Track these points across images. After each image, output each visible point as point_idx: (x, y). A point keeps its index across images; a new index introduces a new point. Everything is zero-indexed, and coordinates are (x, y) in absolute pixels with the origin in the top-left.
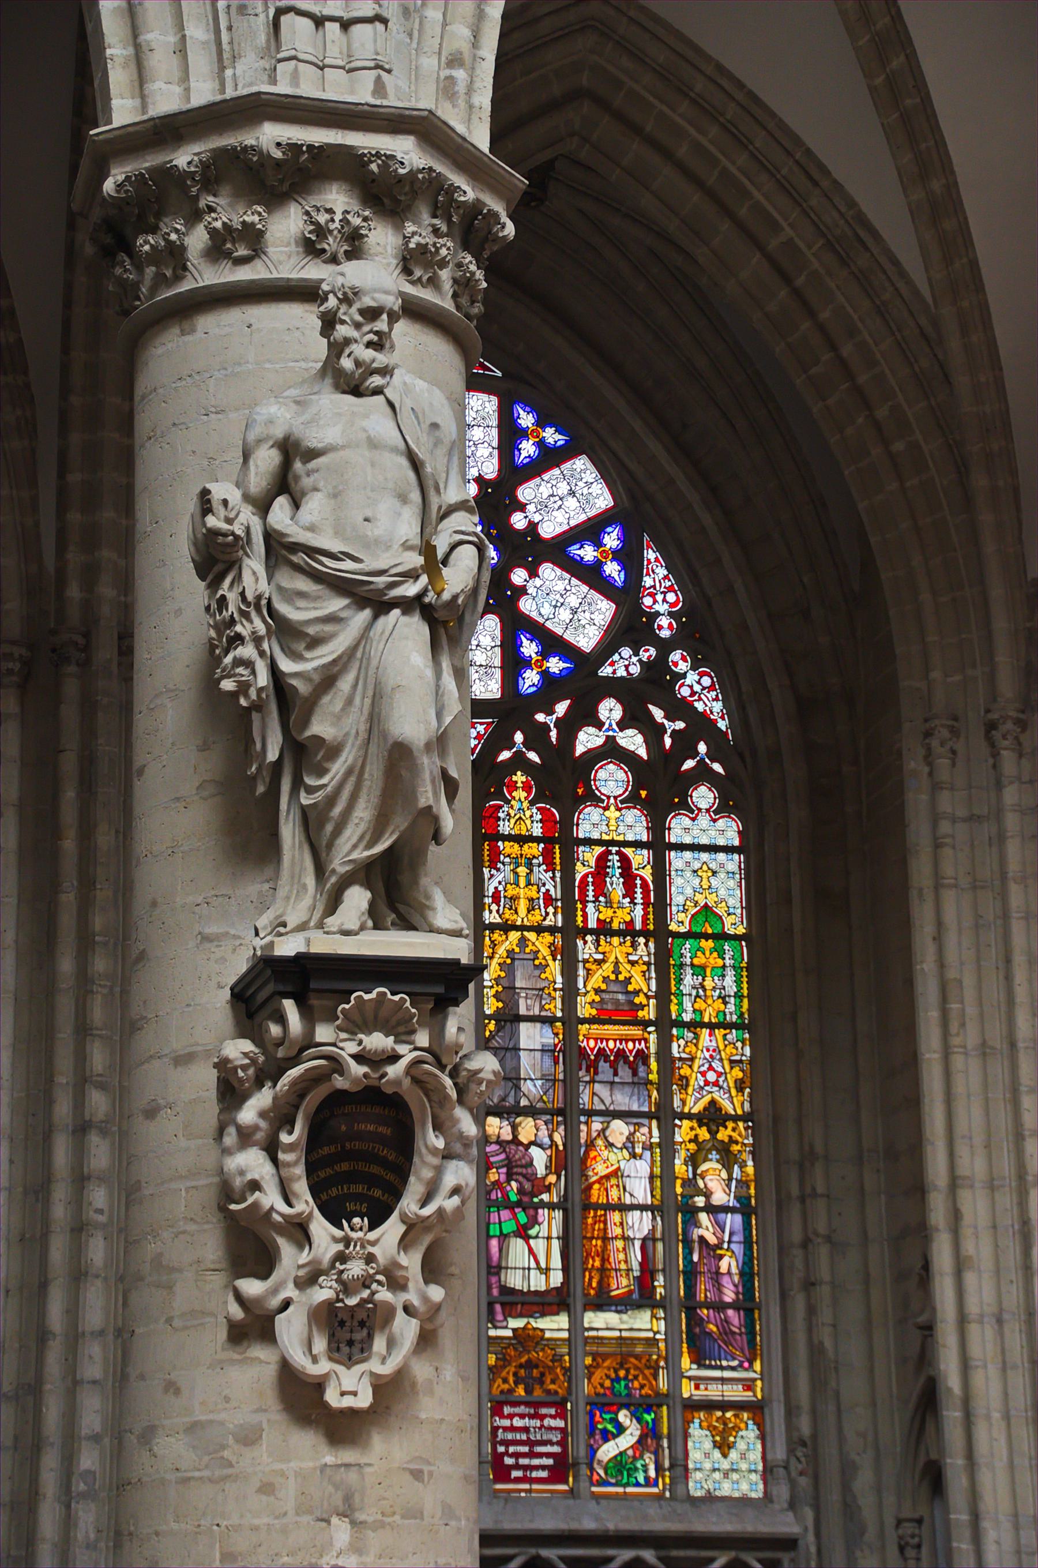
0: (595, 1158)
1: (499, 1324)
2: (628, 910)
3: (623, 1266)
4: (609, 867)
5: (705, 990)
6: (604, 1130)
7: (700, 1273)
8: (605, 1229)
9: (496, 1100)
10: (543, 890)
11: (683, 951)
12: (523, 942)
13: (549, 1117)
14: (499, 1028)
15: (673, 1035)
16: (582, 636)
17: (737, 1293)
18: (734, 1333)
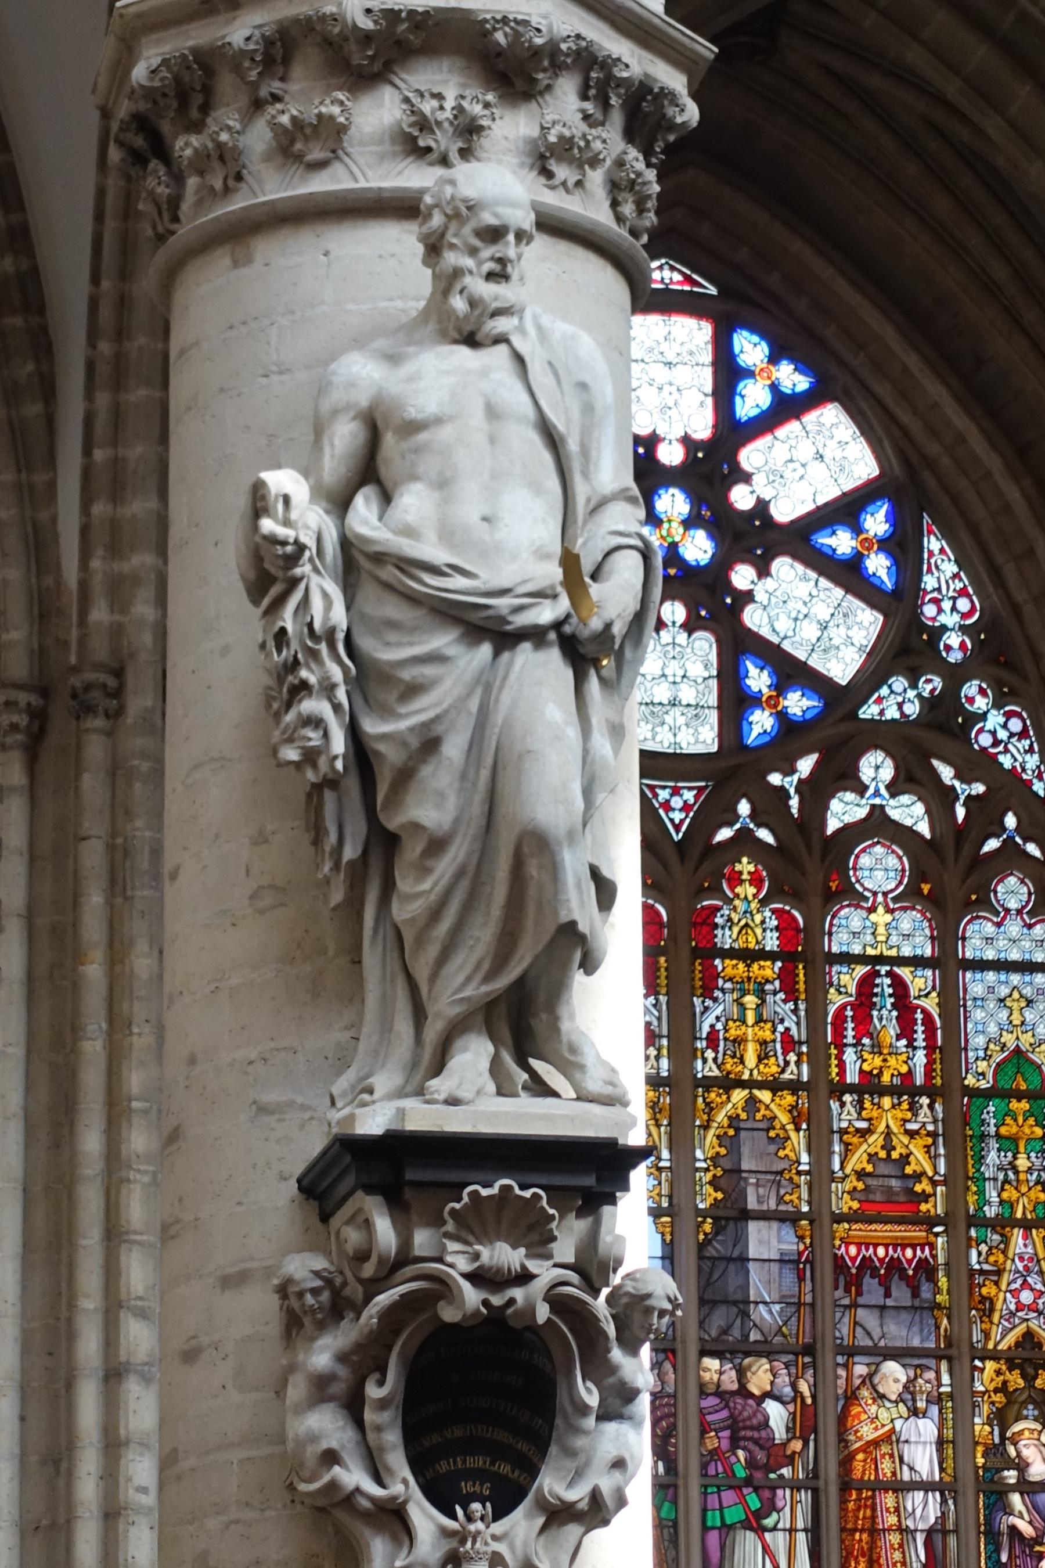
0: (859, 1414)
2: (904, 1057)
4: (876, 995)
5: (1017, 1172)
6: (871, 1376)
8: (874, 1517)
10: (781, 1028)
11: (985, 1116)
12: (752, 1102)
13: (791, 1357)
14: (718, 1229)
16: (834, 660)
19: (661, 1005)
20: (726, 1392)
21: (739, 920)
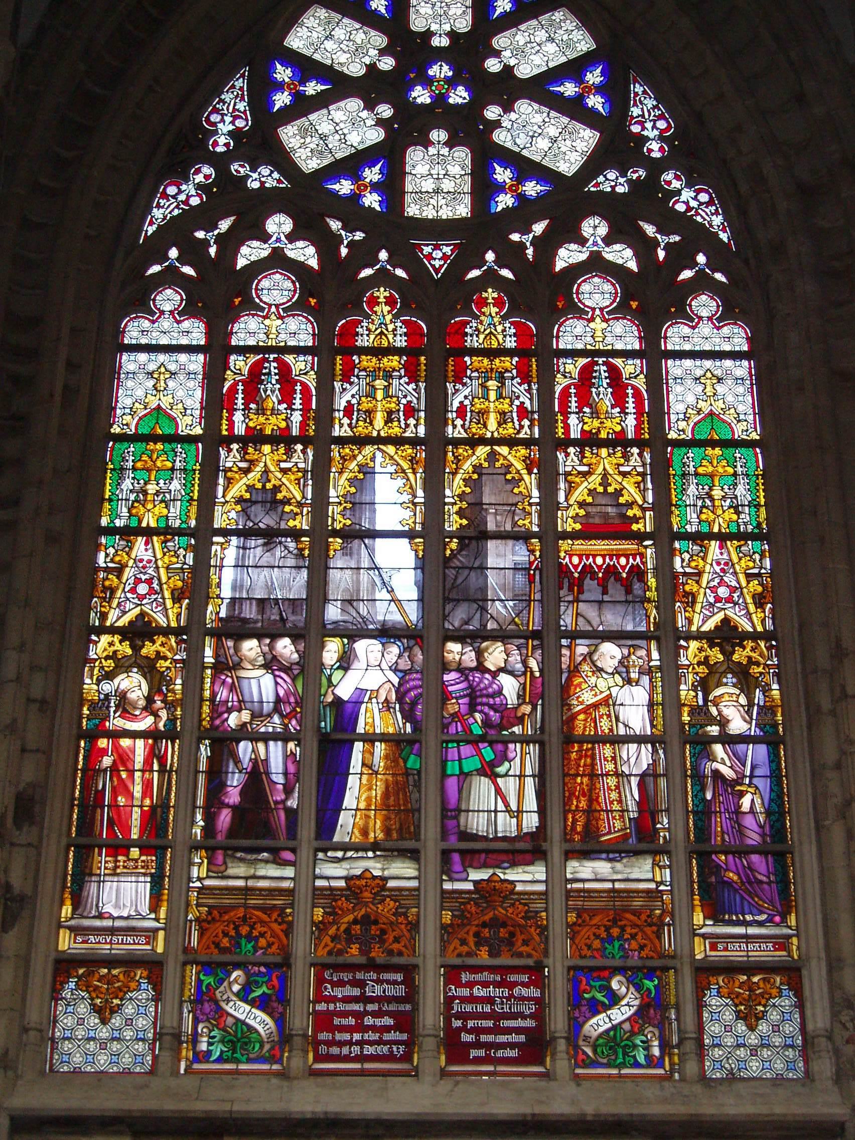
0: (579, 685)
1: (456, 876)
3: (616, 807)
5: (712, 500)
6: (591, 654)
7: (716, 812)
8: (593, 765)
9: (457, 624)
10: (517, 403)
12: (492, 457)
13: (522, 641)
14: (462, 547)
15: (675, 549)
17: (763, 835)
18: (761, 882)
19: (420, 389)
20: (466, 669)
21: (485, 330)
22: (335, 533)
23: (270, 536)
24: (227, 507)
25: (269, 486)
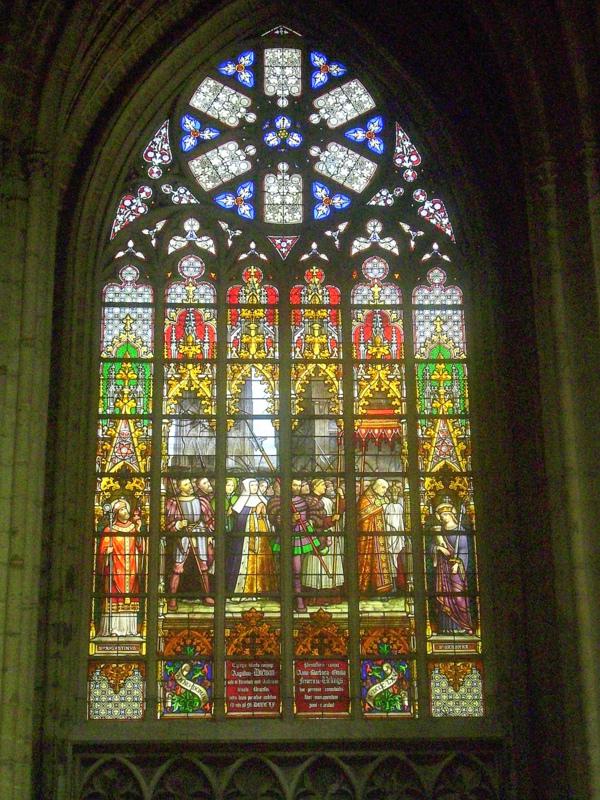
3: (385, 571)
5: (439, 395)
6: (371, 486)
8: (373, 548)
12: (317, 370)
14: (300, 424)
17: (464, 586)
22: (231, 417)
23: (195, 419)
24: (170, 401)
25: (192, 389)
